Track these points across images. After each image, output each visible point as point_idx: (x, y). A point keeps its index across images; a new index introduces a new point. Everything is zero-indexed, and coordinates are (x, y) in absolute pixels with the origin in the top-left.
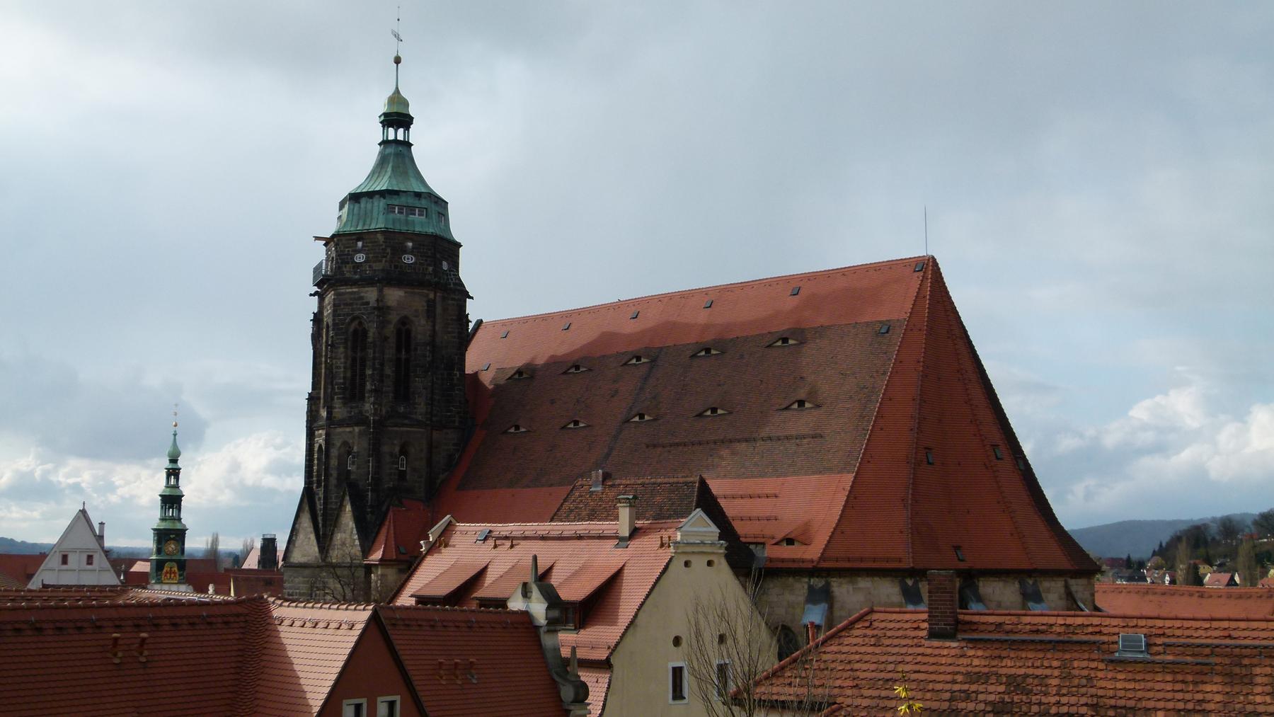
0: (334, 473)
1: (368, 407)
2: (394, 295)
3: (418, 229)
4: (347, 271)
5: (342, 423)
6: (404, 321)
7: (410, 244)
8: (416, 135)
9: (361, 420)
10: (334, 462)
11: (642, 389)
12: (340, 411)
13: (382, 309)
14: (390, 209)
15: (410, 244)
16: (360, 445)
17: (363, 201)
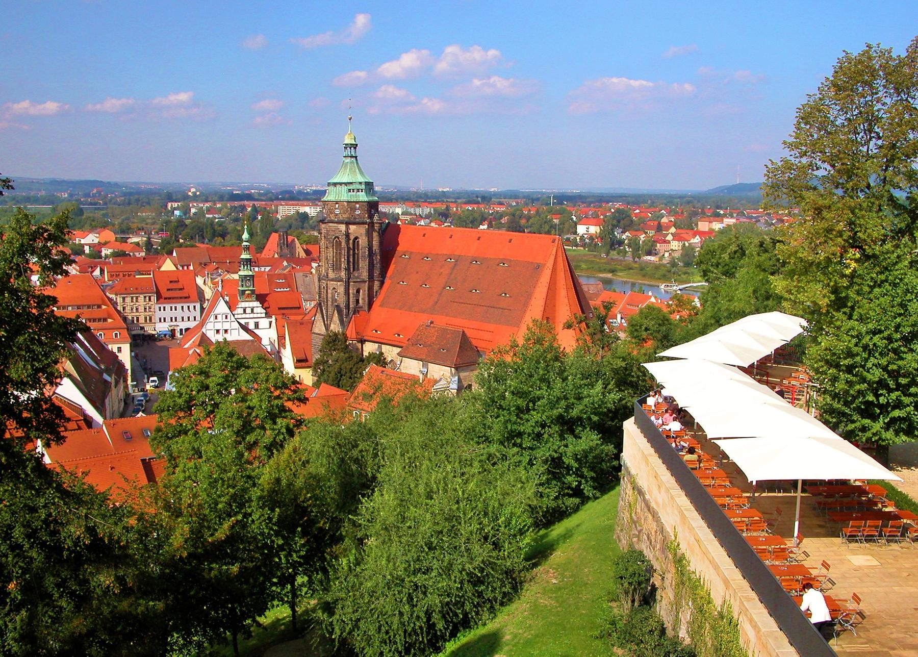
0: (330, 299)
1: (343, 274)
2: (352, 228)
3: (361, 199)
4: (332, 217)
5: (332, 280)
6: (356, 238)
7: (358, 206)
8: (359, 152)
9: (341, 281)
10: (330, 295)
11: (451, 274)
12: (331, 275)
13: (347, 235)
14: (350, 190)
15: (358, 206)
16: (341, 290)
17: (338, 186)
